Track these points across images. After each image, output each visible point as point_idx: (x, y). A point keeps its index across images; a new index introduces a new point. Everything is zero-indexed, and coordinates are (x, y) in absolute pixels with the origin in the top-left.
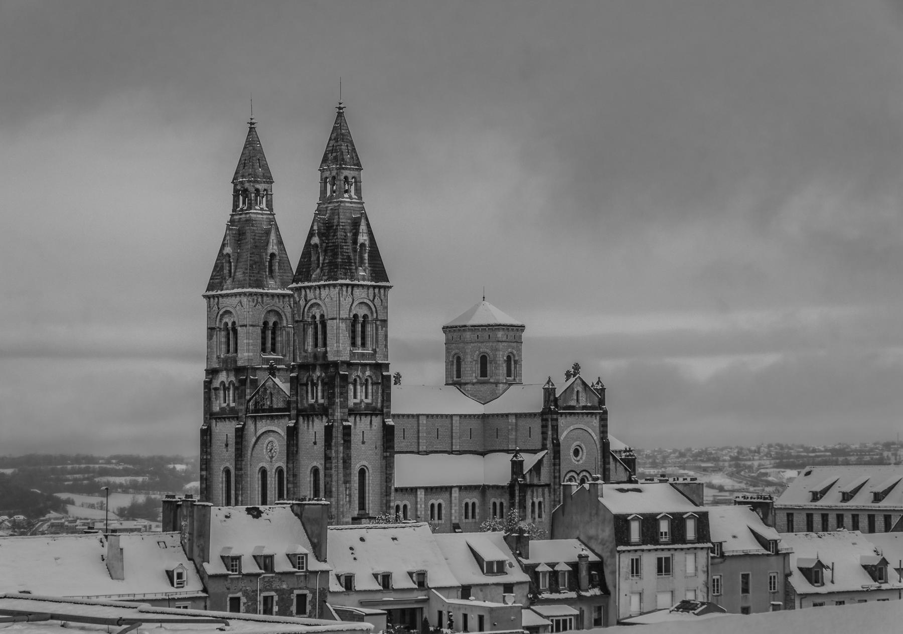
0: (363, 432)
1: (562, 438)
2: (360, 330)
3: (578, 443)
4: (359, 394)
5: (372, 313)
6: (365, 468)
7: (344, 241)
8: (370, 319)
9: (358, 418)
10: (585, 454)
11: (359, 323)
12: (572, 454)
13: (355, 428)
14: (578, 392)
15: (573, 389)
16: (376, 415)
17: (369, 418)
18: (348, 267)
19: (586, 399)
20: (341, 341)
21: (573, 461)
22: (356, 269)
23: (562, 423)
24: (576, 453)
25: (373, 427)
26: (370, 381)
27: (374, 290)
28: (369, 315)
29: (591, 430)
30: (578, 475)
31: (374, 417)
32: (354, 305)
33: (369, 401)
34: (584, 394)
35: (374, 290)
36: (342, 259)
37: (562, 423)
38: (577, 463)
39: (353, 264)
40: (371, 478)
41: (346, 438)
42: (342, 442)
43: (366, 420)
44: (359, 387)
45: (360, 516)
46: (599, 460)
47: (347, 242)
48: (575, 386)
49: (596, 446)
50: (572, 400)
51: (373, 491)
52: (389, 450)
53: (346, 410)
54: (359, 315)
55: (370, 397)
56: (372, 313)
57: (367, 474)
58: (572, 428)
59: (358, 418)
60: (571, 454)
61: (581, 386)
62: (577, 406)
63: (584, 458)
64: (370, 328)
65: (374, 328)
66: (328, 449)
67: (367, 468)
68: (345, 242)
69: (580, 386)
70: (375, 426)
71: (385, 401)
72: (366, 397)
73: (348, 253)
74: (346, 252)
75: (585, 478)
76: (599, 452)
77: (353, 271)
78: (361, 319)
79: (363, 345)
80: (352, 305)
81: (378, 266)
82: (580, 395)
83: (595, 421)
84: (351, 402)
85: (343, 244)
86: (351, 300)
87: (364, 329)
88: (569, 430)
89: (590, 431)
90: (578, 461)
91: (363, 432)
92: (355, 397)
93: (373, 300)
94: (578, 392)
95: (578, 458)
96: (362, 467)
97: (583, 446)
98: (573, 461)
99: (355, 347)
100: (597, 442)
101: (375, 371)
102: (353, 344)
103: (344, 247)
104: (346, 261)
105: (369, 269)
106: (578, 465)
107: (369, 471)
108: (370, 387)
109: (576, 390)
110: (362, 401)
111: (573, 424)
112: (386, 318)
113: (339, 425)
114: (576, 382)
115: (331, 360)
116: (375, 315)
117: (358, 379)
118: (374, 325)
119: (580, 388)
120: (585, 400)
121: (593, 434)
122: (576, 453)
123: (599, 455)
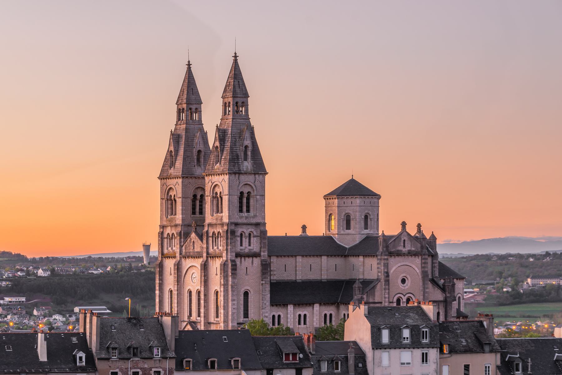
0: (247, 268)
1: (391, 272)
2: (245, 201)
3: (404, 275)
4: (244, 243)
5: (254, 191)
6: (248, 291)
7: (234, 144)
8: (252, 194)
9: (243, 259)
10: (410, 282)
11: (244, 197)
12: (399, 281)
13: (241, 265)
14: (404, 240)
15: (401, 239)
16: (256, 257)
17: (251, 259)
18: (236, 162)
19: (411, 245)
20: (231, 210)
21: (401, 287)
22: (242, 162)
23: (392, 261)
24: (403, 281)
25: (254, 265)
26: (252, 235)
27: (255, 176)
28: (252, 192)
29: (414, 266)
30: (404, 296)
31: (254, 258)
32: (240, 186)
33: (250, 248)
34: (409, 242)
35: (255, 176)
36: (232, 156)
37: (392, 261)
38: (403, 288)
39: (240, 159)
40: (252, 297)
41: (233, 272)
42: (231, 274)
43: (249, 260)
44: (244, 239)
45: (244, 322)
46: (421, 286)
47: (236, 145)
48: (402, 236)
49: (419, 277)
50: (400, 246)
51: (254, 306)
52: (264, 280)
53: (234, 254)
54: (244, 192)
55: (252, 245)
56: (254, 191)
57: (250, 295)
58: (399, 265)
59: (243, 259)
60: (399, 282)
61: (407, 237)
62: (404, 250)
63: (409, 285)
64: (252, 201)
65: (255, 201)
66: (222, 279)
67: (250, 291)
68: (235, 145)
69: (406, 237)
70: (256, 264)
71: (262, 248)
72: (250, 245)
73: (237, 152)
74: (235, 152)
75: (410, 298)
76: (421, 280)
77: (240, 164)
78: (246, 195)
79: (248, 211)
80: (238, 186)
81: (258, 160)
82: (406, 243)
83: (418, 260)
84: (239, 248)
85: (234, 146)
86: (238, 182)
87: (249, 201)
88: (397, 266)
89: (414, 266)
90: (404, 287)
91: (247, 268)
92: (241, 245)
93: (254, 182)
94: (404, 240)
95: (405, 285)
96: (246, 290)
97: (408, 276)
98: (401, 287)
99: (242, 212)
100: (420, 274)
101: (255, 228)
102: (241, 211)
103: (234, 148)
104: (235, 157)
105: (252, 162)
106: (404, 289)
107: (251, 293)
108: (252, 239)
109: (403, 239)
110: (246, 247)
111: (400, 262)
112: (263, 194)
113: (229, 263)
114: (403, 234)
115: (225, 221)
116: (255, 192)
117: (243, 234)
118: (255, 199)
119: (406, 239)
120: (410, 246)
121: (416, 269)
122: (403, 281)
123: (421, 282)
